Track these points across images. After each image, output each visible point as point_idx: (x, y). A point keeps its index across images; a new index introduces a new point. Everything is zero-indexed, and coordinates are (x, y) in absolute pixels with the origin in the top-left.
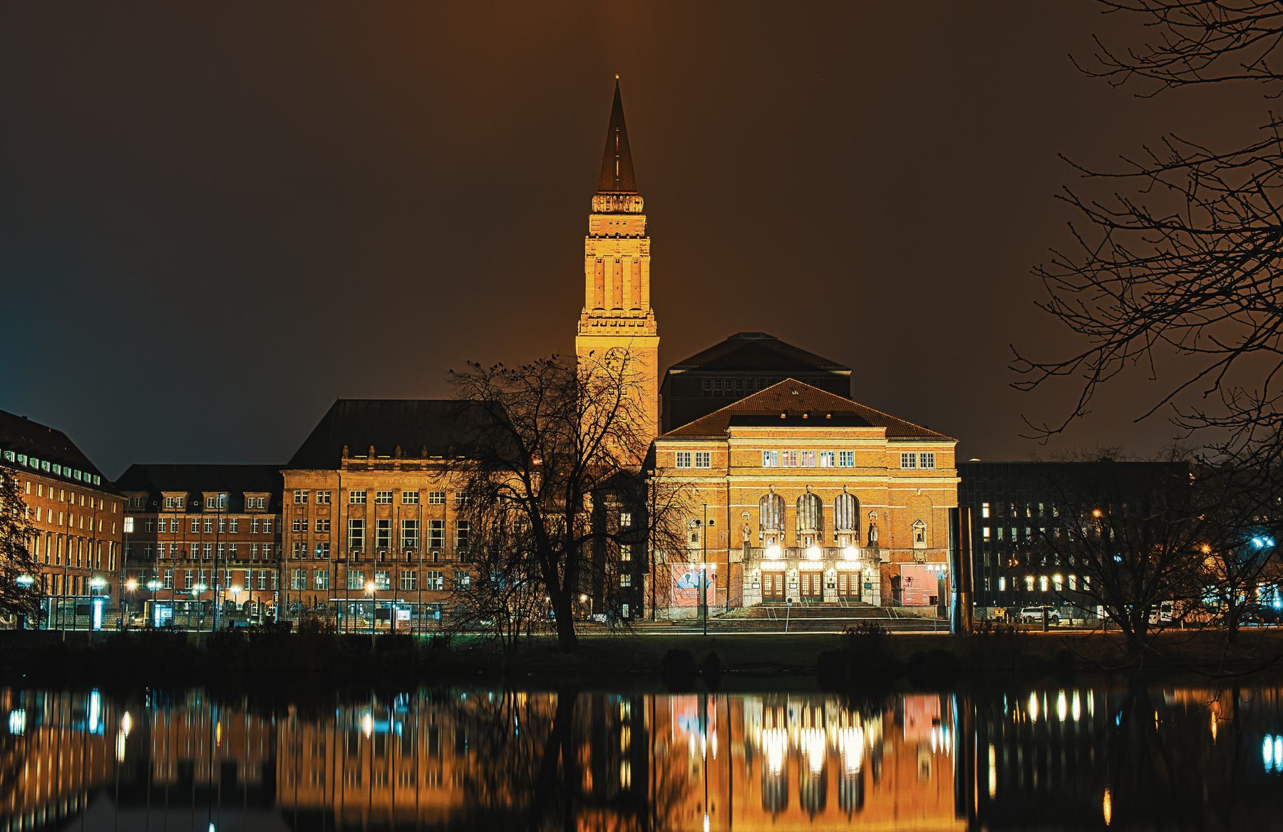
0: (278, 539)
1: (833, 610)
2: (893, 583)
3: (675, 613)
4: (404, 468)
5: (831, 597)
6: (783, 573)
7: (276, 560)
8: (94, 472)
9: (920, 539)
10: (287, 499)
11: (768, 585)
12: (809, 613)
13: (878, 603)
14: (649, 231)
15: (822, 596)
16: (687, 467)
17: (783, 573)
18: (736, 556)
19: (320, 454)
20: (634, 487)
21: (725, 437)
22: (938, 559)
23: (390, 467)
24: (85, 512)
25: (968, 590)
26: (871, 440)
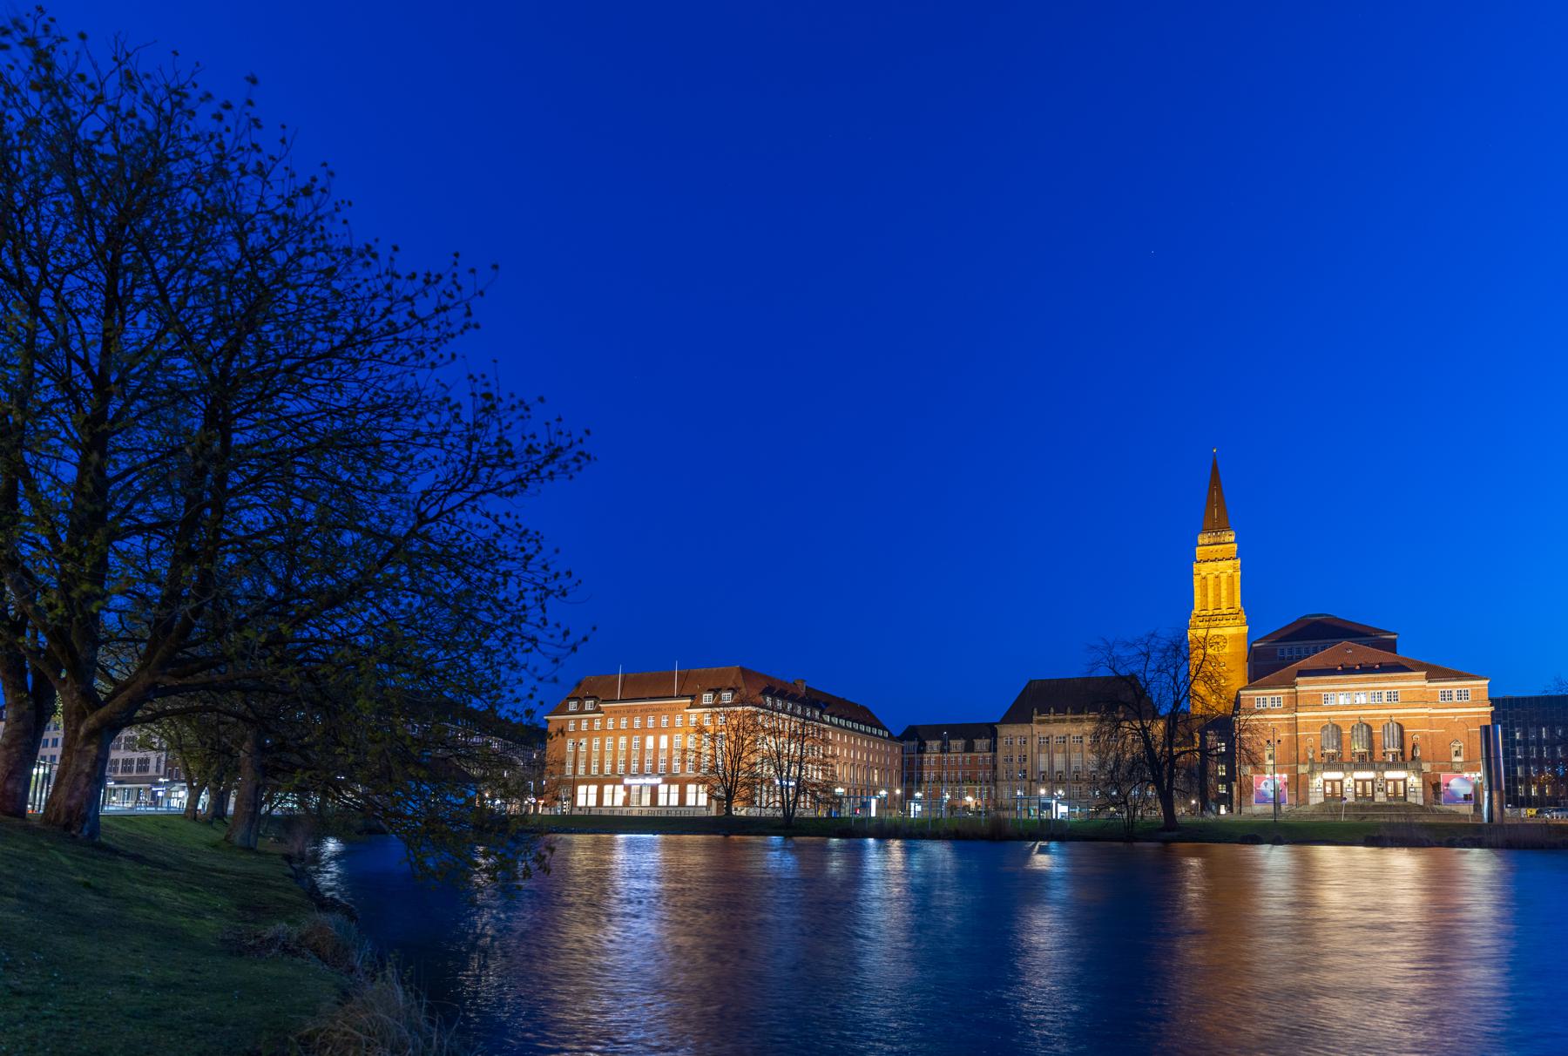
0: (995, 767)
1: (1382, 806)
2: (1434, 787)
3: (1258, 808)
4: (1072, 721)
5: (1380, 798)
6: (1341, 781)
7: (995, 780)
8: (884, 729)
9: (1457, 754)
10: (1001, 743)
11: (1328, 789)
12: (1362, 807)
13: (1421, 802)
14: (1239, 554)
15: (1373, 798)
16: (1268, 709)
17: (1341, 781)
18: (1302, 769)
19: (1020, 713)
20: (1224, 725)
21: (1294, 685)
22: (1475, 769)
23: (1064, 721)
24: (879, 753)
25: (1499, 787)
26: (1415, 683)
